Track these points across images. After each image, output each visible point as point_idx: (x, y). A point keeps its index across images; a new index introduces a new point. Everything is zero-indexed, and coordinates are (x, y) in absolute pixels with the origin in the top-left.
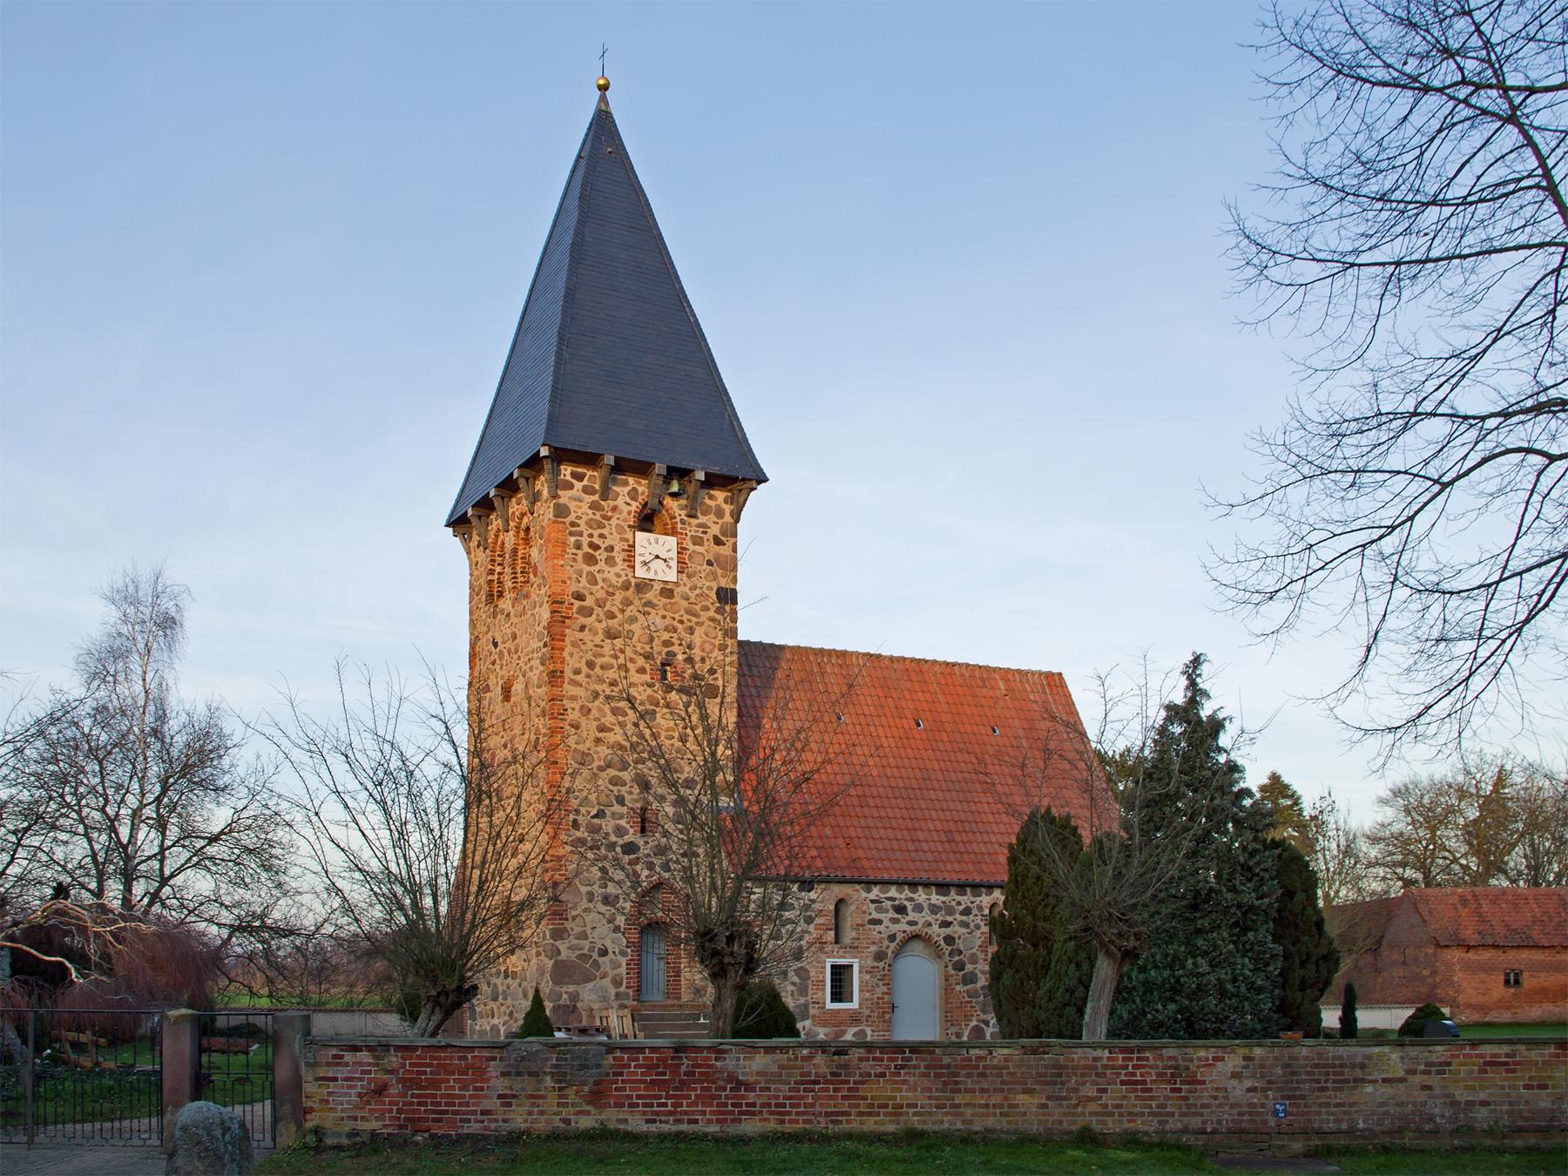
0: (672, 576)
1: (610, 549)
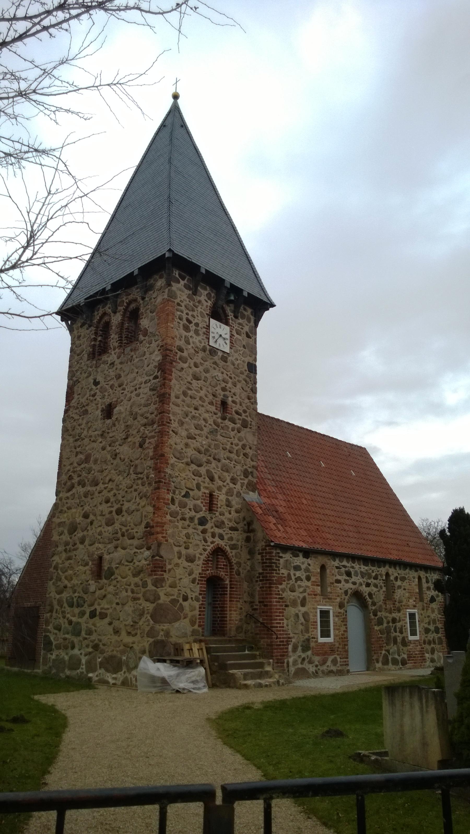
0: (227, 349)
1: (197, 325)
